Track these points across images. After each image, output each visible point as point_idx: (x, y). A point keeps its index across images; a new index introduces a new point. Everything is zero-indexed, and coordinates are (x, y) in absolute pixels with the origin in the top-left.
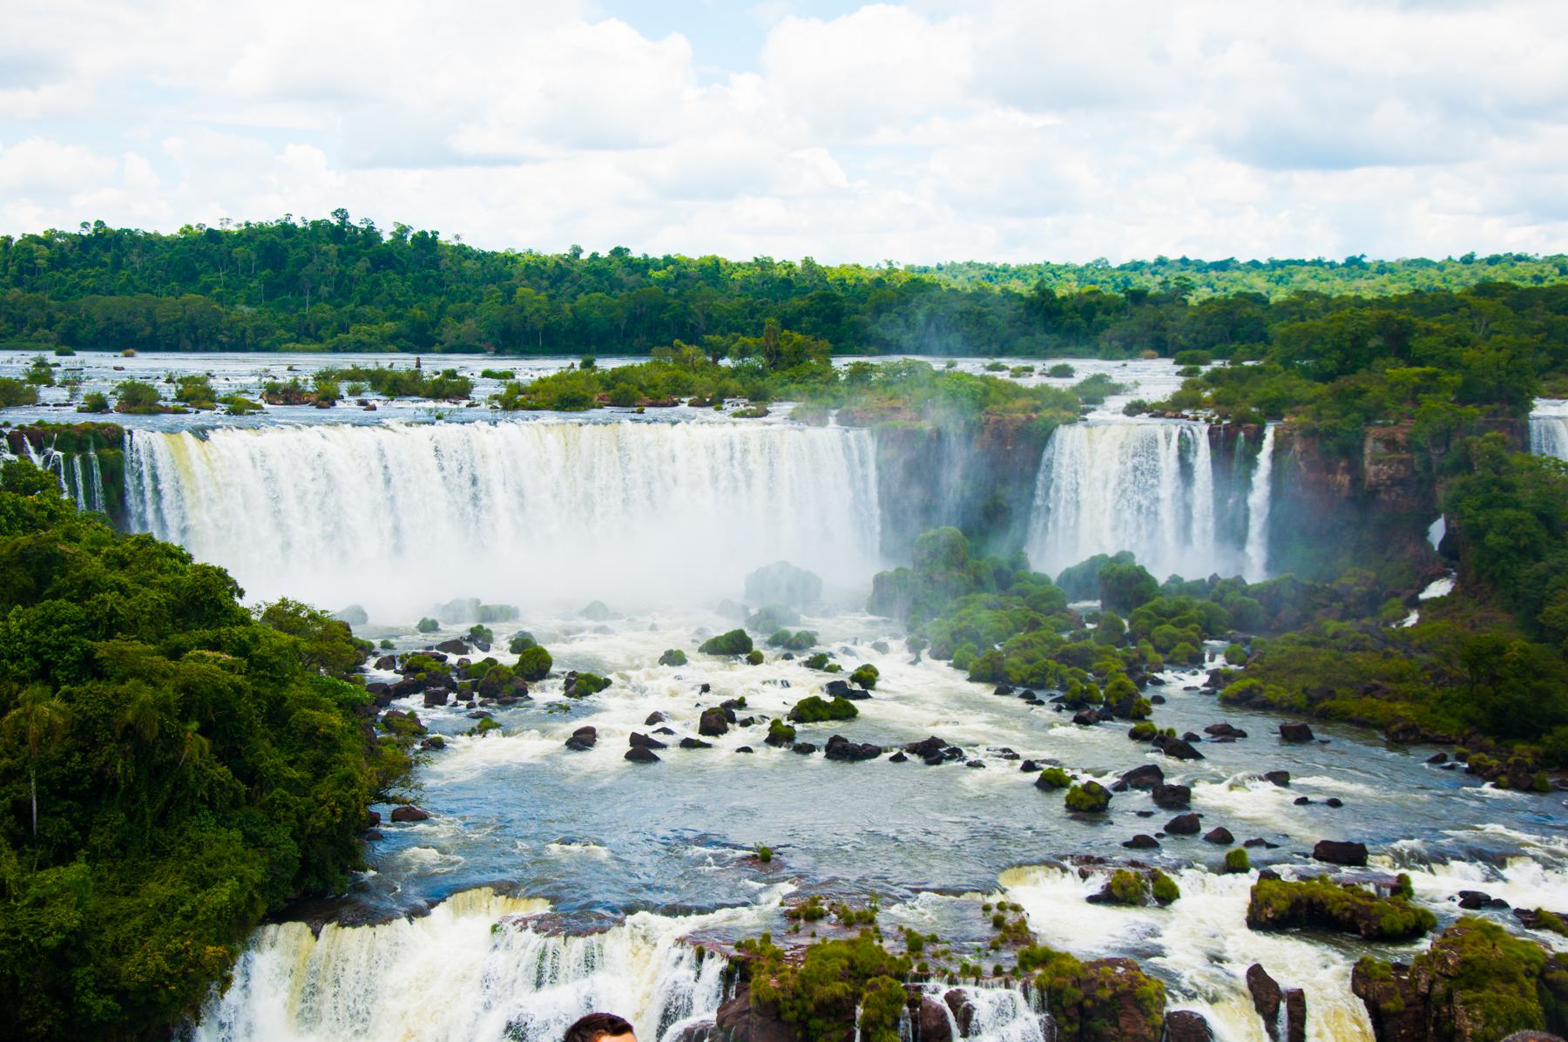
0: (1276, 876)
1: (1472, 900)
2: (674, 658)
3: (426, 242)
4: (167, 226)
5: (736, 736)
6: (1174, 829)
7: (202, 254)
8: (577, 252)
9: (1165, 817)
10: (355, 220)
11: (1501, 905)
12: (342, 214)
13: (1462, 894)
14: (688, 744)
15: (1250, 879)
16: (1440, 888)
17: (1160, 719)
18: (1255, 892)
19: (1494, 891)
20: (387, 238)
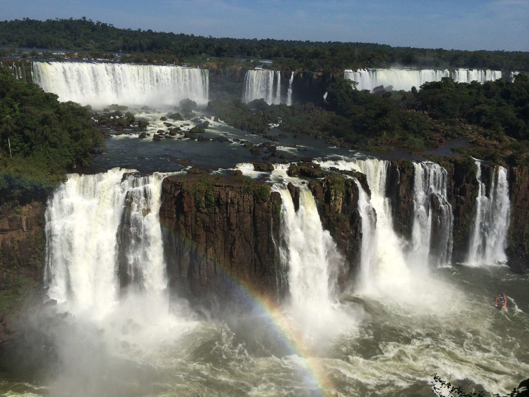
0: (294, 164)
1: (332, 169)
2: (163, 119)
3: (104, 25)
4: (44, 20)
5: (178, 135)
6: (273, 155)
7: (52, 26)
8: (140, 30)
9: (271, 153)
10: (87, 19)
11: (338, 169)
12: (84, 18)
13: (330, 168)
14: (166, 137)
15: (288, 165)
16: (326, 165)
17: (269, 134)
18: (289, 168)
19: (336, 167)
20: (95, 24)
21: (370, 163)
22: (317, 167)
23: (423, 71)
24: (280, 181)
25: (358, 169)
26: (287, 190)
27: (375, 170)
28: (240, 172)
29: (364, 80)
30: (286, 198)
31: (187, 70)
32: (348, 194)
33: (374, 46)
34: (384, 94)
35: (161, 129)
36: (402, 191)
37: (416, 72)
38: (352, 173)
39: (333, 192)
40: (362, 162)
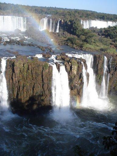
16: (70, 55)
19: (75, 56)
21: (87, 55)
22: (67, 56)
23: (108, 22)
24: (53, 61)
25: (83, 58)
26: (55, 65)
27: (89, 59)
28: (37, 57)
29: (86, 25)
30: (54, 67)
31: (18, 18)
32: (79, 67)
33: (76, 11)
34: (93, 30)
35: (7, 40)
36: (99, 67)
37: (106, 22)
38: (81, 59)
39: (73, 66)
40: (85, 55)
